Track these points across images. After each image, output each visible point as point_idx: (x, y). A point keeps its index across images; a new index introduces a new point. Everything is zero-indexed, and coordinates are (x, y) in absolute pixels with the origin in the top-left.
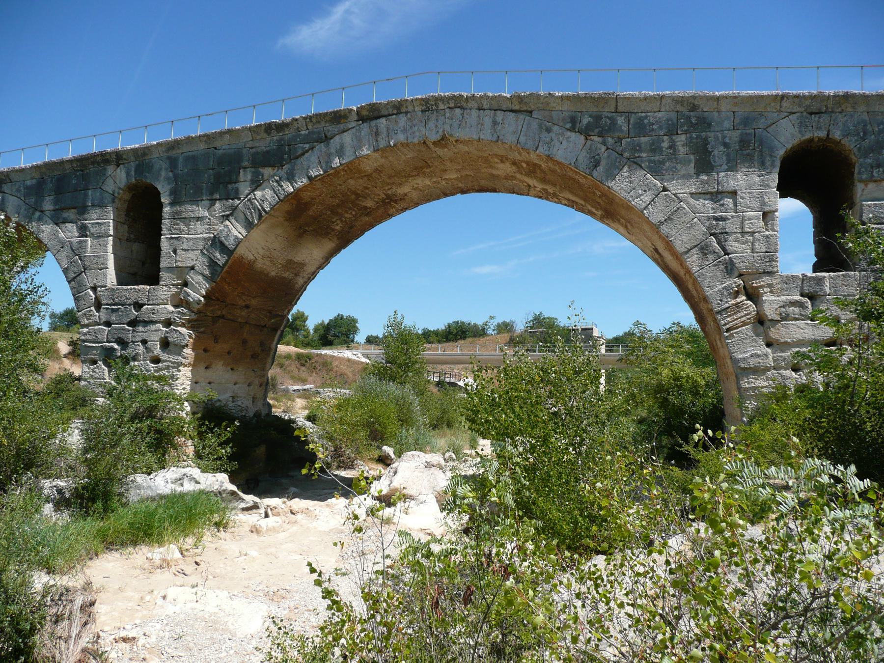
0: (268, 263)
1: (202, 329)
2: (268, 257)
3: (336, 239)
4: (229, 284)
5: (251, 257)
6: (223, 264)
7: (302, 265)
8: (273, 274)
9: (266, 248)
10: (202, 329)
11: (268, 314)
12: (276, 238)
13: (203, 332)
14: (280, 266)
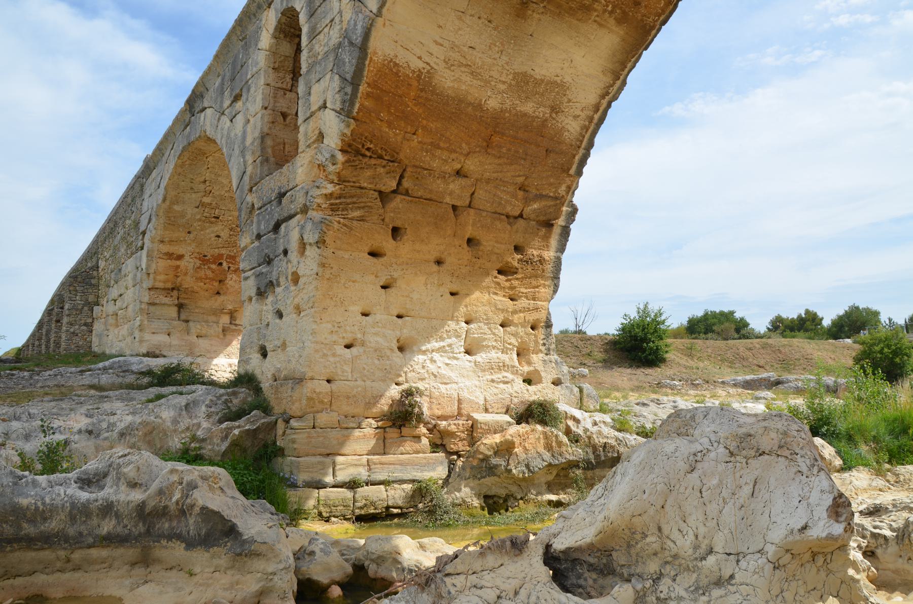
0: (467, 78)
1: (357, 214)
2: (461, 65)
3: (612, 21)
4: (390, 125)
5: (416, 64)
6: (353, 78)
7: (558, 87)
8: (493, 104)
9: (446, 44)
10: (357, 214)
11: (521, 194)
12: (460, 19)
13: (361, 219)
14: (503, 87)
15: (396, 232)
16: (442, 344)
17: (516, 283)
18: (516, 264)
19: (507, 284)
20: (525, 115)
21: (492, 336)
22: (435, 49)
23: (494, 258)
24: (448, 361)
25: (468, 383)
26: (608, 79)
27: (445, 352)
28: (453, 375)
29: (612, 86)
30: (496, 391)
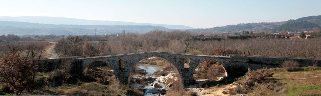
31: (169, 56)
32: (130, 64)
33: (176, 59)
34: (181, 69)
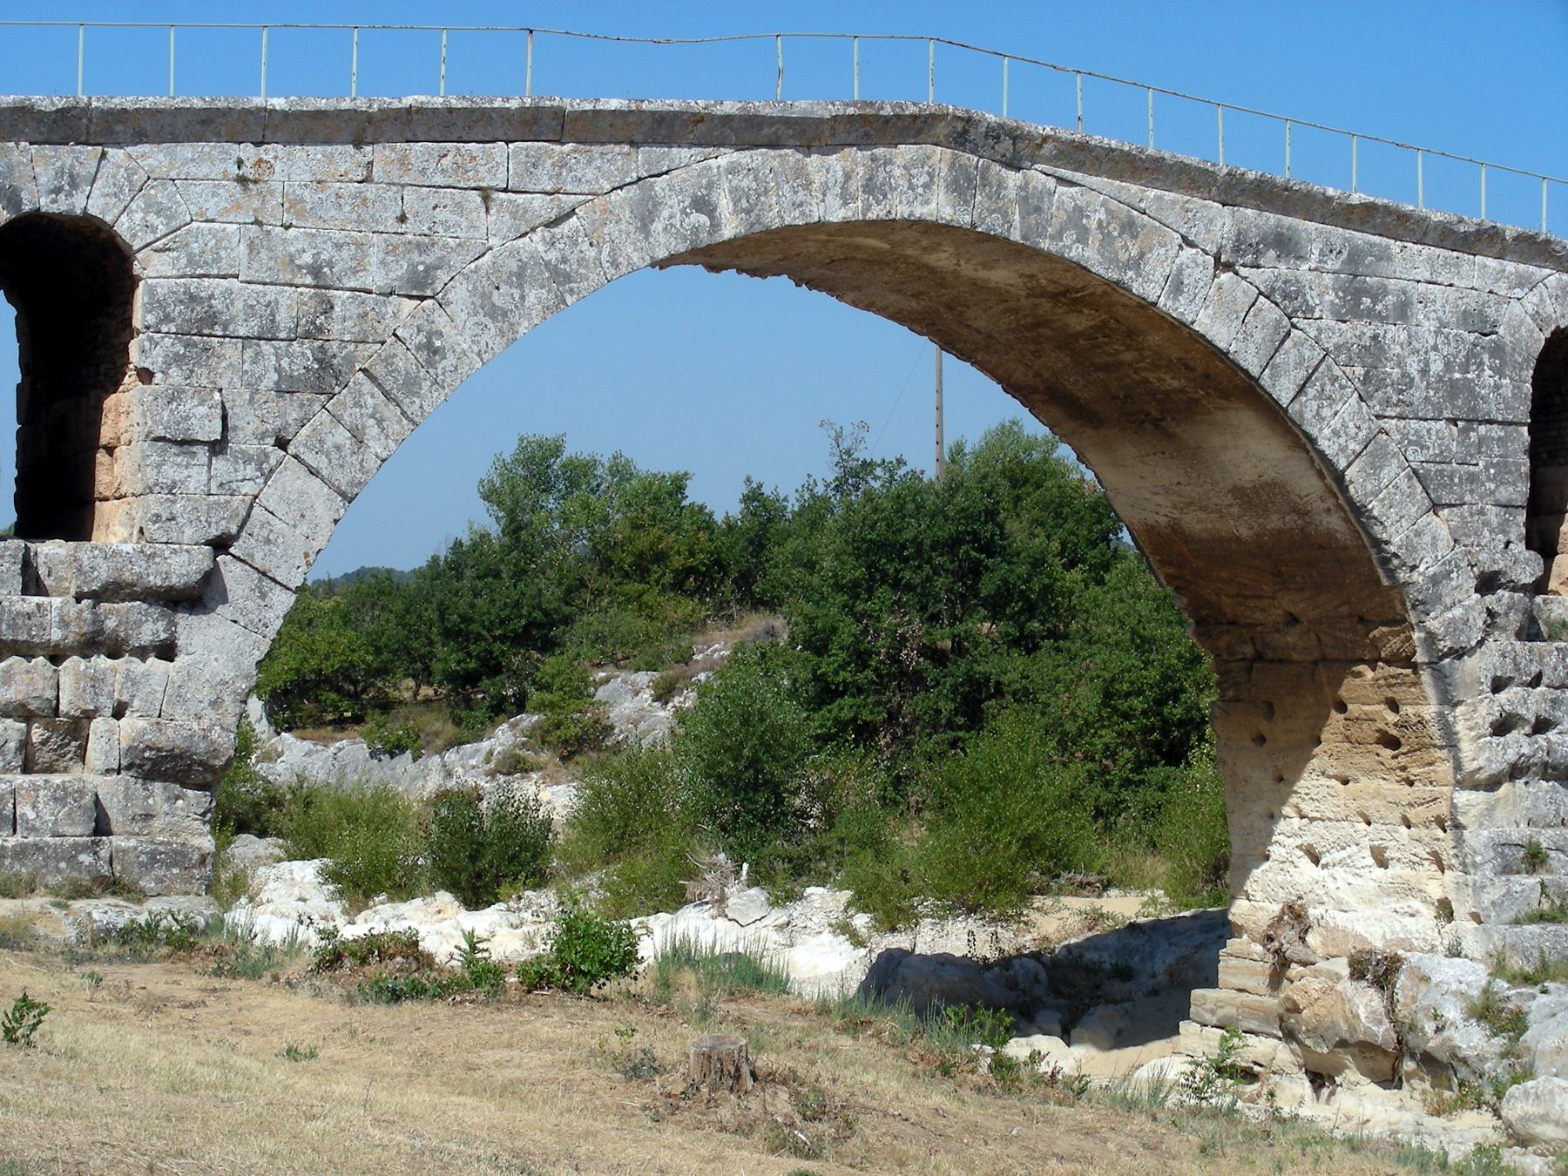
15: (1270, 711)
16: (1343, 854)
17: (1403, 760)
18: (1394, 732)
19: (1394, 763)
20: (1280, 532)
21: (1394, 842)
22: (1158, 499)
23: (1365, 726)
24: (1351, 879)
25: (1368, 913)
26: (1303, 455)
27: (1348, 865)
28: (1352, 901)
29: (1312, 461)
30: (1398, 927)
31: (1240, 244)
32: (286, 388)
33: (1394, 334)
34: (1488, 583)
